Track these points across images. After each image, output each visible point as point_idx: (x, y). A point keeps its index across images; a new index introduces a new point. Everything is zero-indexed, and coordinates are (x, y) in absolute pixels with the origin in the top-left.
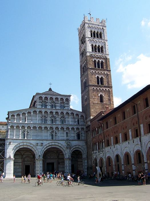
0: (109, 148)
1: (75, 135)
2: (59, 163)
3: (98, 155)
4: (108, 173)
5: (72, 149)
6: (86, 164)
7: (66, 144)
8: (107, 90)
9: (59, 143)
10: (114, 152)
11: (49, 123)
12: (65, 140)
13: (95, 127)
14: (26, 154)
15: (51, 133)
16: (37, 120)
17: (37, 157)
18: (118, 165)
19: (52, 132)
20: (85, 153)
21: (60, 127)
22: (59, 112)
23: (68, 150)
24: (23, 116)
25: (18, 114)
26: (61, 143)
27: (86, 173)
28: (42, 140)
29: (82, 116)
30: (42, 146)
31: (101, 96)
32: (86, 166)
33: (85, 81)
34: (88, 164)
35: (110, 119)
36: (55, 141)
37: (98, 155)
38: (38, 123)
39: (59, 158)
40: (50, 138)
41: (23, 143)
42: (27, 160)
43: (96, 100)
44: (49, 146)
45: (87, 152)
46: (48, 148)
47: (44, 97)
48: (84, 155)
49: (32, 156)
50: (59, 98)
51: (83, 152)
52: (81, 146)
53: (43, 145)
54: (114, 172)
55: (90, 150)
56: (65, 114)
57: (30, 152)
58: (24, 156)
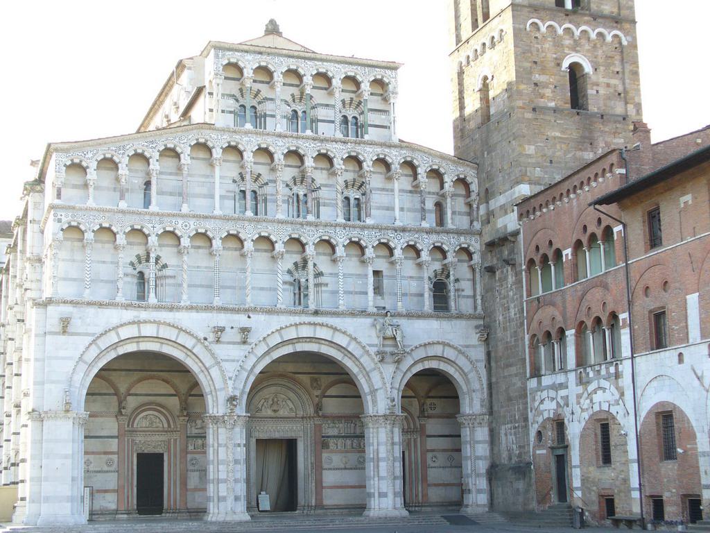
0: (667, 357)
1: (427, 286)
2: (322, 443)
3: (579, 397)
4: (658, 504)
5: (409, 361)
6: (482, 450)
7: (373, 333)
8: (609, 38)
9: (335, 329)
11: (281, 216)
12: (369, 315)
13: (551, 243)
14: (140, 388)
15: (289, 272)
16: (212, 196)
17: (216, 406)
19: (296, 264)
20: (476, 386)
21: (341, 239)
22: (339, 152)
23: (389, 369)
24: (136, 171)
25: (105, 159)
26: (350, 331)
27: (483, 499)
28: (248, 311)
29: (462, 182)
30: (244, 342)
31: (574, 69)
32: (478, 458)
34: (492, 450)
35: (684, 194)
37: (579, 397)
38: (218, 212)
39: (324, 417)
40: (285, 298)
41: (139, 323)
42: (145, 423)
43: (548, 92)
44: (284, 343)
45: (490, 386)
46: (276, 354)
47: (249, 64)
48: (472, 400)
49: (174, 402)
50: (337, 73)
51: (467, 382)
52: (455, 348)
53: (252, 339)
55: (513, 370)
56: (367, 166)
57: (167, 382)
58: (129, 398)
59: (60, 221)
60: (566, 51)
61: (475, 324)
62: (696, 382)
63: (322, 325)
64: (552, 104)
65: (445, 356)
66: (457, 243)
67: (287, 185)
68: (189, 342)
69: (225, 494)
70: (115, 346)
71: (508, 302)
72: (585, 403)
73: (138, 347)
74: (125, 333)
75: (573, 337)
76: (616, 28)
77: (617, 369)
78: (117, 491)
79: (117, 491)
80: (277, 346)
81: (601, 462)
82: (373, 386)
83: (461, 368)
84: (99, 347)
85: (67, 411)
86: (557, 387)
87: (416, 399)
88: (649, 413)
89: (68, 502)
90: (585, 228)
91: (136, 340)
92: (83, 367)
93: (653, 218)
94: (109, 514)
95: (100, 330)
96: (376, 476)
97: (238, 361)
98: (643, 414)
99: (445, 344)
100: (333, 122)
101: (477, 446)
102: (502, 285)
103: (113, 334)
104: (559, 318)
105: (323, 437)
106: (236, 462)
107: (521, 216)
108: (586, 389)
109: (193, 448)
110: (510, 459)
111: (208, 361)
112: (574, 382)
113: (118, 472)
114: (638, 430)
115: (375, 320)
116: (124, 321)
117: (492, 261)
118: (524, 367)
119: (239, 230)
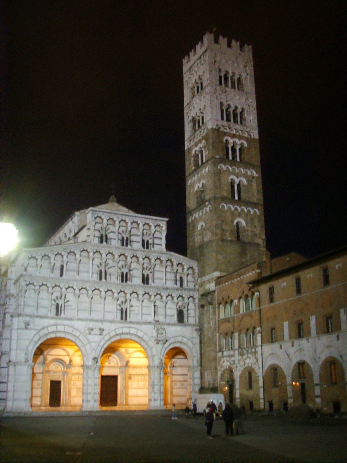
0: (275, 346)
3: (239, 360)
4: (271, 405)
5: (168, 343)
9: (138, 329)
10: (291, 357)
13: (229, 297)
18: (303, 386)
20: (195, 354)
23: (160, 346)
30: (101, 334)
33: (200, 186)
34: (201, 383)
35: (283, 282)
36: (131, 325)
41: (56, 325)
43: (228, 234)
44: (117, 335)
45: (201, 355)
46: (113, 340)
51: (192, 352)
54: (290, 401)
55: (211, 348)
59: (25, 281)
60: (235, 216)
62: (287, 356)
63: (132, 328)
64: (229, 239)
67: (119, 268)
68: (77, 334)
70: (46, 335)
71: (209, 320)
72: (242, 363)
74: (51, 329)
75: (238, 336)
76: (255, 208)
77: (255, 349)
80: (114, 336)
81: (248, 388)
83: (189, 347)
85: (26, 362)
86: (230, 356)
88: (269, 367)
90: (243, 292)
92: (32, 344)
93: (271, 290)
95: (40, 328)
97: (97, 342)
98: (265, 369)
99: (183, 337)
100: (139, 242)
102: (207, 313)
104: (232, 328)
106: (95, 385)
107: (216, 285)
108: (242, 358)
109: (74, 378)
110: (209, 385)
111: (85, 342)
112: (237, 355)
113: (41, 388)
114: (264, 374)
117: (203, 302)
118: (216, 348)
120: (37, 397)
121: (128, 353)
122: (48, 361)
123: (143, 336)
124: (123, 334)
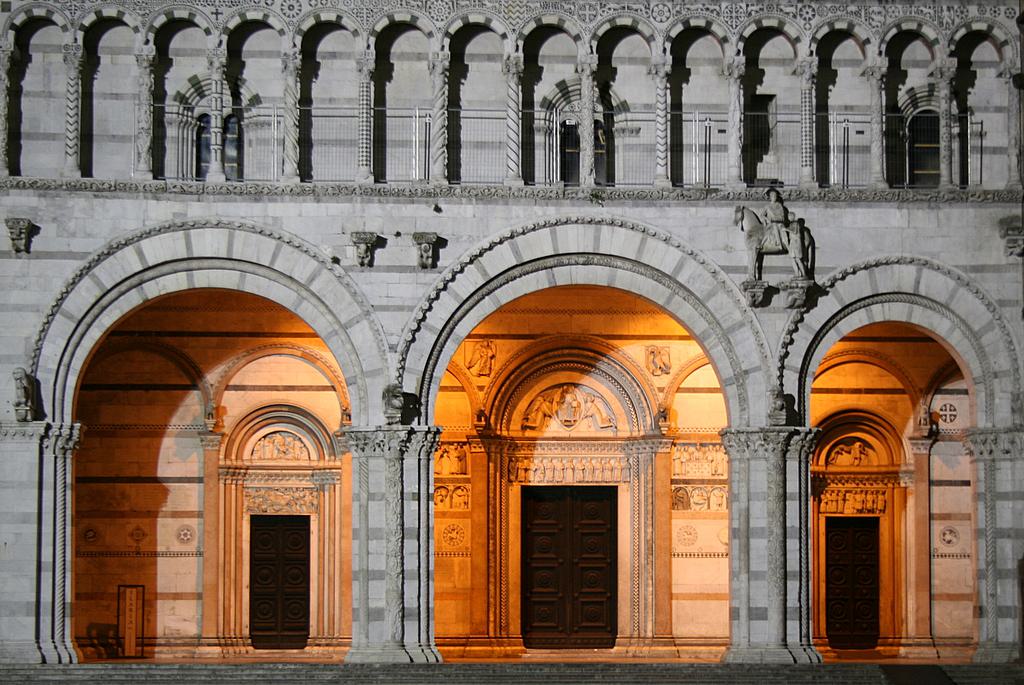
5: (826, 306)
26: (681, 234)
48: (991, 395)
53: (448, 258)
61: (1001, 216)
65: (923, 294)
66: (957, 21)
68: (302, 268)
69: (382, 604)
70: (137, 279)
73: (190, 279)
74: (157, 249)
78: (199, 596)
79: (199, 596)
80: (507, 275)
82: (738, 364)
84: (99, 283)
87: (906, 396)
89: (28, 615)
91: (184, 265)
92: (61, 327)
94: (184, 645)
95: (97, 246)
96: (744, 570)
97: (411, 309)
101: (999, 504)
103: (129, 251)
105: (673, 482)
111: (347, 310)
115: (741, 210)
116: (151, 224)
119: (417, 13)
120: (177, 596)
121: (665, 370)
122: (228, 422)
123: (679, 267)
124: (559, 258)
